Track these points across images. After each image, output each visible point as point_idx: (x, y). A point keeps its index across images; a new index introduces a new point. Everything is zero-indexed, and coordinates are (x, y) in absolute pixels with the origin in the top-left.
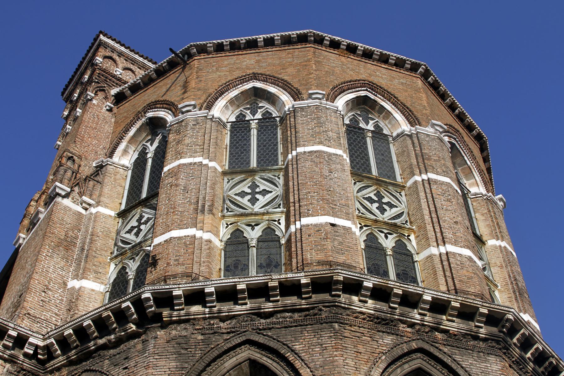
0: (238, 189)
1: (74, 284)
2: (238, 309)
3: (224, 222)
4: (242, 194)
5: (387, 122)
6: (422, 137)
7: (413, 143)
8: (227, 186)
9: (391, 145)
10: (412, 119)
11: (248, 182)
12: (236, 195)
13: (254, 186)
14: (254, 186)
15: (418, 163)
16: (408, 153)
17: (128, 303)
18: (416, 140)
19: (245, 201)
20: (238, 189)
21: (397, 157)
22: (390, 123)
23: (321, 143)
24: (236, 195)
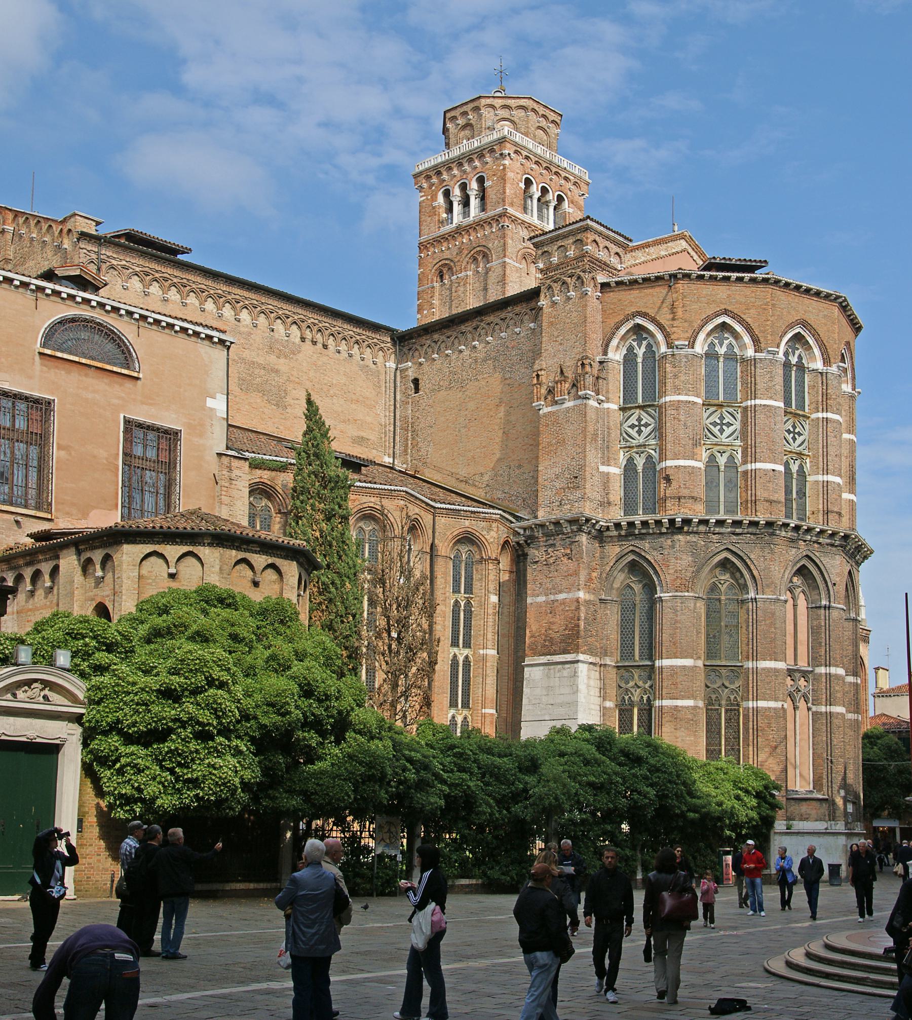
0: (711, 420)
1: (603, 469)
2: (723, 530)
3: (704, 447)
4: (715, 424)
5: (807, 352)
6: (829, 376)
7: (822, 379)
8: (705, 415)
9: (806, 375)
10: (827, 361)
11: (718, 414)
12: (710, 424)
13: (722, 418)
14: (722, 418)
15: (822, 401)
16: (818, 389)
17: (667, 520)
18: (824, 378)
19: (716, 430)
20: (711, 420)
21: (809, 389)
22: (809, 354)
23: (771, 398)
24: (710, 424)
